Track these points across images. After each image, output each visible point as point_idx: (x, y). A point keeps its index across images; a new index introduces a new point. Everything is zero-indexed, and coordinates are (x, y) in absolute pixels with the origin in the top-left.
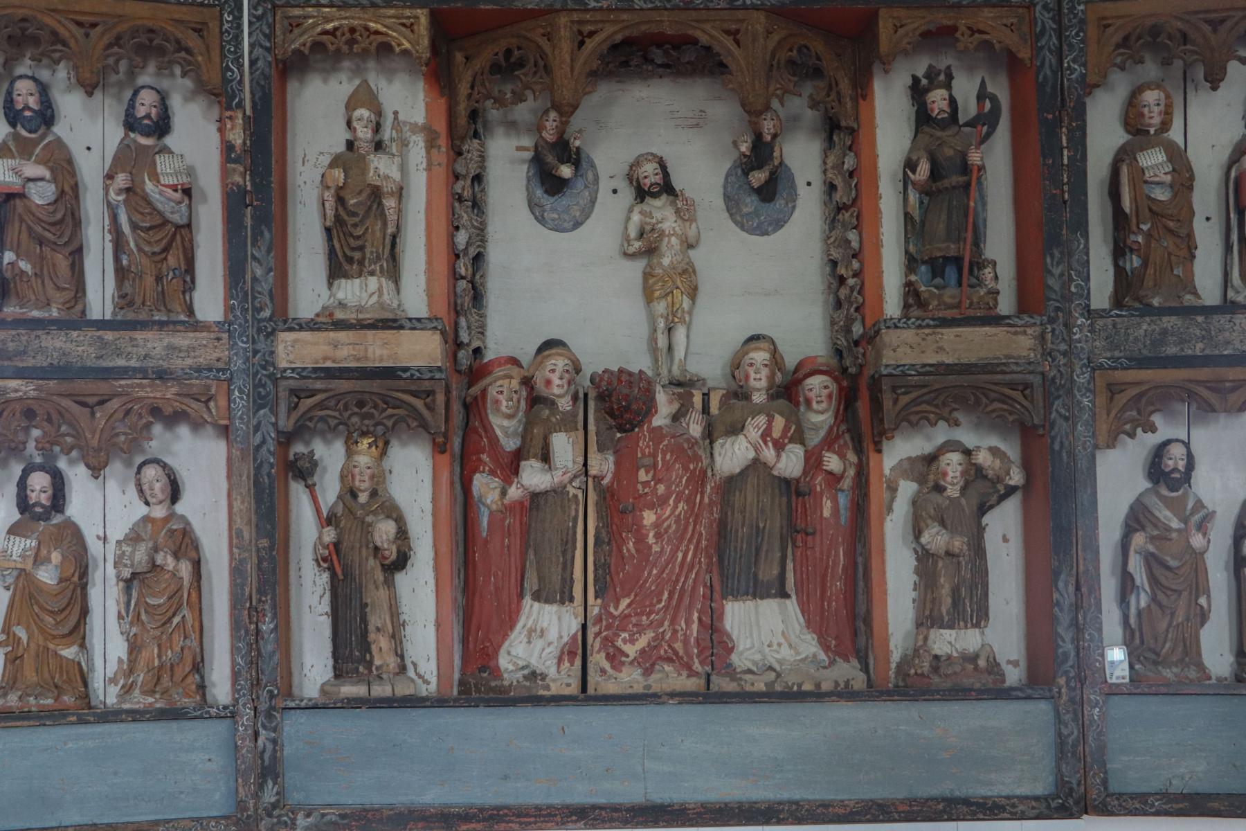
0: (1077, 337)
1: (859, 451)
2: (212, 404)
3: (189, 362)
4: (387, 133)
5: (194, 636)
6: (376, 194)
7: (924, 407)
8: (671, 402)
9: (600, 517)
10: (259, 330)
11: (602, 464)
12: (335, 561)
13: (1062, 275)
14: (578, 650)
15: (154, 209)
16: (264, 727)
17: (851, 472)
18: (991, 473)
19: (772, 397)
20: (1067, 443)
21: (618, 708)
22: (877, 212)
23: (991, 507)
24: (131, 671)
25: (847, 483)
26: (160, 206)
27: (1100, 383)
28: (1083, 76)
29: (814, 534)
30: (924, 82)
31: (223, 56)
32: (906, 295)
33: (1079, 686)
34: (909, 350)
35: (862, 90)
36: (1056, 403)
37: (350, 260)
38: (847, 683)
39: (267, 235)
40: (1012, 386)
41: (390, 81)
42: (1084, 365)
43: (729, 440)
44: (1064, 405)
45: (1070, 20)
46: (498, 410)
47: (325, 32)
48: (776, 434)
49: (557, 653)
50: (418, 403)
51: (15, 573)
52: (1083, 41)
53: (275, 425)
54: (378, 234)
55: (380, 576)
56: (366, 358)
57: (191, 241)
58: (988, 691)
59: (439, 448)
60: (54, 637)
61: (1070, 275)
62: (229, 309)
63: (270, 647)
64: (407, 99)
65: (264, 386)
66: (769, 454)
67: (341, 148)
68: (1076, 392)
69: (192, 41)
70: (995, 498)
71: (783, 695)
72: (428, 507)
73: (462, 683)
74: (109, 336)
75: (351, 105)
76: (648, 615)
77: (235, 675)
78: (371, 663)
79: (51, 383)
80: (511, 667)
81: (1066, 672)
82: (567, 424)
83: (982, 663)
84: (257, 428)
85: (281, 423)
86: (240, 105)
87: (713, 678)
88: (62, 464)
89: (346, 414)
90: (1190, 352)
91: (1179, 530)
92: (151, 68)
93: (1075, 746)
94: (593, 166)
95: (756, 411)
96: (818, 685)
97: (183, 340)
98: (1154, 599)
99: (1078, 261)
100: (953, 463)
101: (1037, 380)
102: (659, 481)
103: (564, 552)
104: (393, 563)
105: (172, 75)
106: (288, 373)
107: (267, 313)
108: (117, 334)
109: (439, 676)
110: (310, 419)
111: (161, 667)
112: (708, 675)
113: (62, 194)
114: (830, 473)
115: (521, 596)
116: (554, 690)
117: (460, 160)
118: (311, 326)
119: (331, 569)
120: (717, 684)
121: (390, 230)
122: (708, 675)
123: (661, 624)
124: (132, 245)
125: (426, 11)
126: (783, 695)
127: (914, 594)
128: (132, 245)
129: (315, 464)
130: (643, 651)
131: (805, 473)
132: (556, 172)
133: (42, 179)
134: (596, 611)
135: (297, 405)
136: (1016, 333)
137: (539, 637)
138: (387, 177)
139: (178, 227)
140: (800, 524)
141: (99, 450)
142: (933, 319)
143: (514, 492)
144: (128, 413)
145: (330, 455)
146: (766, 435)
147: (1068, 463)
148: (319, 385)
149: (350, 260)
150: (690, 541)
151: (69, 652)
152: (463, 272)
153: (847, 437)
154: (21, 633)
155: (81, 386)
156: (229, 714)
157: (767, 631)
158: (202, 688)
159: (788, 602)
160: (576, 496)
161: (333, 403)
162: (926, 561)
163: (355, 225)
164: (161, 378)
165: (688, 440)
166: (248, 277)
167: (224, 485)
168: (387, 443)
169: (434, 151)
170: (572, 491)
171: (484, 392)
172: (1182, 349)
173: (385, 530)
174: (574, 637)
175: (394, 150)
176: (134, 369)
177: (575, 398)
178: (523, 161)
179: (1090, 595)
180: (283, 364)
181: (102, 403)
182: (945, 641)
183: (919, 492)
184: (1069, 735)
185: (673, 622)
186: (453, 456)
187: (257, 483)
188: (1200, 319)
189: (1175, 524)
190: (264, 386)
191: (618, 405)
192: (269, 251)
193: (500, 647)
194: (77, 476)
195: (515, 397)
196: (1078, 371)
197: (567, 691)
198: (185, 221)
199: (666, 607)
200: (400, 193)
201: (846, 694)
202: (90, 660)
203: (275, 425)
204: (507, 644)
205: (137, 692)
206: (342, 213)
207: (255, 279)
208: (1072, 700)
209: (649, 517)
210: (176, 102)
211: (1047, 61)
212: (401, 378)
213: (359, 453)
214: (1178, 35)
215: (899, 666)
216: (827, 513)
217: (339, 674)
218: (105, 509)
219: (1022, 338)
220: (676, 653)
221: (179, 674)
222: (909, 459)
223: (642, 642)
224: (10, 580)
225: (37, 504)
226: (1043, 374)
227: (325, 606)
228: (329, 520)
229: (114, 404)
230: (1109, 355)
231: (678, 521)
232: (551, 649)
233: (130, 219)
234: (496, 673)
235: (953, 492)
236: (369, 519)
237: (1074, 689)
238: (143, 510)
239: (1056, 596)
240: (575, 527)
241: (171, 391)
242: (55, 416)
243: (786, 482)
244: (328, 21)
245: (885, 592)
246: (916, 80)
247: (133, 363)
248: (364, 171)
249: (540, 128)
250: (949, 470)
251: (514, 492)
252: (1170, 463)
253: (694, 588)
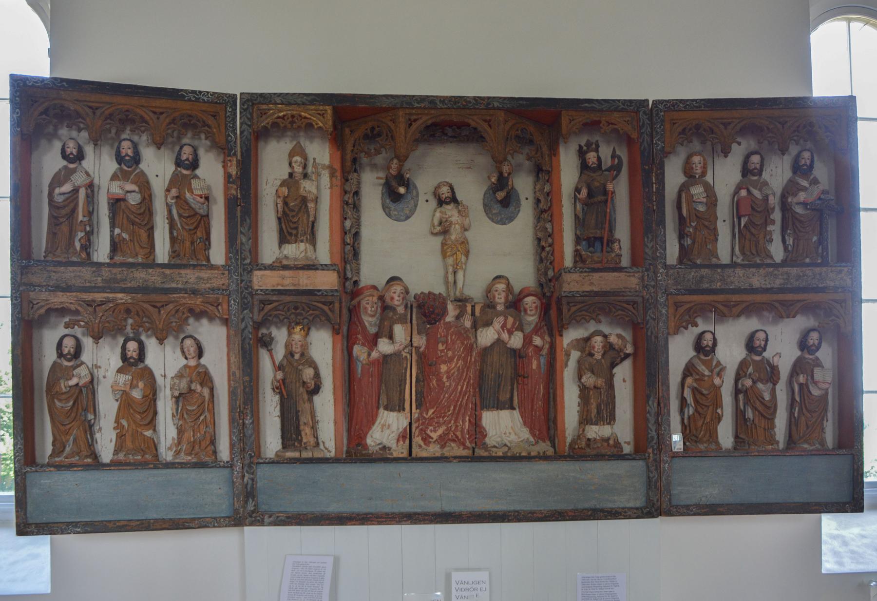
1: (551, 335)
2: (220, 307)
3: (208, 285)
4: (310, 169)
5: (211, 426)
6: (304, 200)
7: (584, 313)
8: (455, 309)
9: (418, 368)
10: (244, 270)
11: (420, 341)
12: (283, 389)
13: (652, 247)
14: (407, 435)
15: (191, 207)
16: (247, 472)
17: (547, 346)
18: (617, 347)
19: (507, 308)
21: (428, 464)
22: (561, 214)
23: (617, 364)
24: (179, 443)
25: (544, 352)
26: (193, 206)
29: (527, 377)
30: (585, 148)
31: (226, 129)
32: (575, 256)
35: (554, 151)
37: (291, 234)
38: (544, 453)
39: (248, 220)
40: (628, 303)
41: (311, 143)
43: (485, 329)
46: (367, 312)
47: (279, 117)
48: (509, 326)
49: (396, 437)
50: (326, 308)
51: (121, 393)
52: (663, 130)
53: (252, 318)
54: (305, 221)
55: (306, 397)
56: (299, 285)
57: (209, 223)
58: (613, 456)
59: (336, 331)
60: (141, 425)
62: (228, 258)
63: (250, 432)
64: (320, 152)
65: (246, 298)
66: (505, 336)
67: (286, 176)
69: (211, 121)
70: (619, 360)
71: (512, 457)
72: (330, 362)
73: (347, 452)
74: (168, 272)
75: (291, 155)
76: (443, 418)
77: (232, 446)
78: (301, 440)
79: (139, 295)
80: (373, 444)
81: (652, 447)
82: (402, 320)
83: (611, 442)
84: (243, 320)
85: (255, 317)
86: (235, 154)
87: (476, 450)
88: (143, 338)
89: (288, 314)
91: (708, 376)
92: (189, 135)
93: (656, 482)
94: (416, 187)
95: (498, 314)
96: (529, 453)
97: (205, 274)
98: (696, 410)
100: (598, 341)
101: (640, 300)
102: (449, 350)
103: (400, 385)
104: (312, 390)
105: (200, 138)
106: (259, 292)
107: (248, 261)
108: (172, 271)
109: (336, 448)
110: (270, 316)
111: (194, 442)
112: (474, 449)
113: (144, 199)
114: (536, 346)
115: (378, 408)
116: (395, 455)
117: (348, 184)
118: (271, 267)
119: (281, 393)
120: (479, 452)
121: (311, 219)
122: (474, 449)
123: (450, 422)
124: (179, 225)
125: (331, 107)
126: (512, 457)
127: (578, 409)
128: (179, 225)
129: (272, 339)
130: (440, 436)
131: (523, 346)
132: (397, 191)
133: (134, 191)
134: (417, 415)
135: (263, 308)
136: (629, 276)
137: (387, 428)
138: (310, 192)
139: (202, 216)
140: (521, 372)
141: (162, 330)
143: (375, 355)
144: (177, 311)
145: (280, 335)
146: (503, 327)
148: (275, 298)
149: (291, 234)
150: (465, 380)
151: (148, 433)
152: (348, 241)
153: (545, 328)
154: (124, 423)
155: (154, 297)
156: (230, 466)
157: (503, 426)
158: (215, 452)
159: (514, 412)
160: (406, 357)
161: (281, 308)
162: (585, 392)
163: (293, 216)
164: (193, 293)
165: (464, 329)
166: (238, 242)
167: (225, 350)
168: (309, 329)
169: (334, 179)
170: (404, 354)
171: (359, 303)
173: (308, 373)
174: (405, 429)
175: (314, 178)
176: (180, 289)
177: (406, 307)
178: (380, 185)
180: (256, 287)
181: (162, 306)
182: (594, 431)
183: (581, 356)
185: (456, 421)
186: (343, 335)
187: (243, 348)
188: (719, 270)
189: (707, 373)
190: (246, 298)
191: (428, 310)
192: (249, 230)
193: (367, 433)
194: (151, 344)
195: (375, 306)
196: (660, 295)
197: (401, 456)
198: (206, 213)
199: (453, 414)
200: (316, 200)
201: (544, 457)
202: (158, 438)
203: (252, 318)
204: (371, 432)
205: (182, 454)
206: (286, 209)
207: (242, 243)
208: (655, 460)
209: (444, 368)
210: (201, 152)
212: (316, 295)
213: (295, 333)
215: (570, 445)
216: (534, 367)
217: (285, 446)
218: (164, 360)
219: (632, 279)
220: (457, 437)
221: (203, 445)
222: (577, 340)
223: (440, 431)
224: (118, 396)
225: (131, 357)
226: (643, 297)
227: (277, 412)
228: (280, 368)
229: (171, 306)
231: (458, 370)
232: (393, 435)
233: (178, 212)
234: (366, 447)
235: (598, 356)
236: (300, 367)
238: (184, 362)
239: (648, 408)
240: (406, 373)
241: (199, 301)
242: (141, 313)
243: (514, 352)
244: (280, 111)
245: (563, 407)
246: (580, 147)
247: (179, 286)
248: (298, 188)
249: (389, 168)
250: (596, 345)
251: (375, 355)
252: (705, 342)
253: (467, 404)
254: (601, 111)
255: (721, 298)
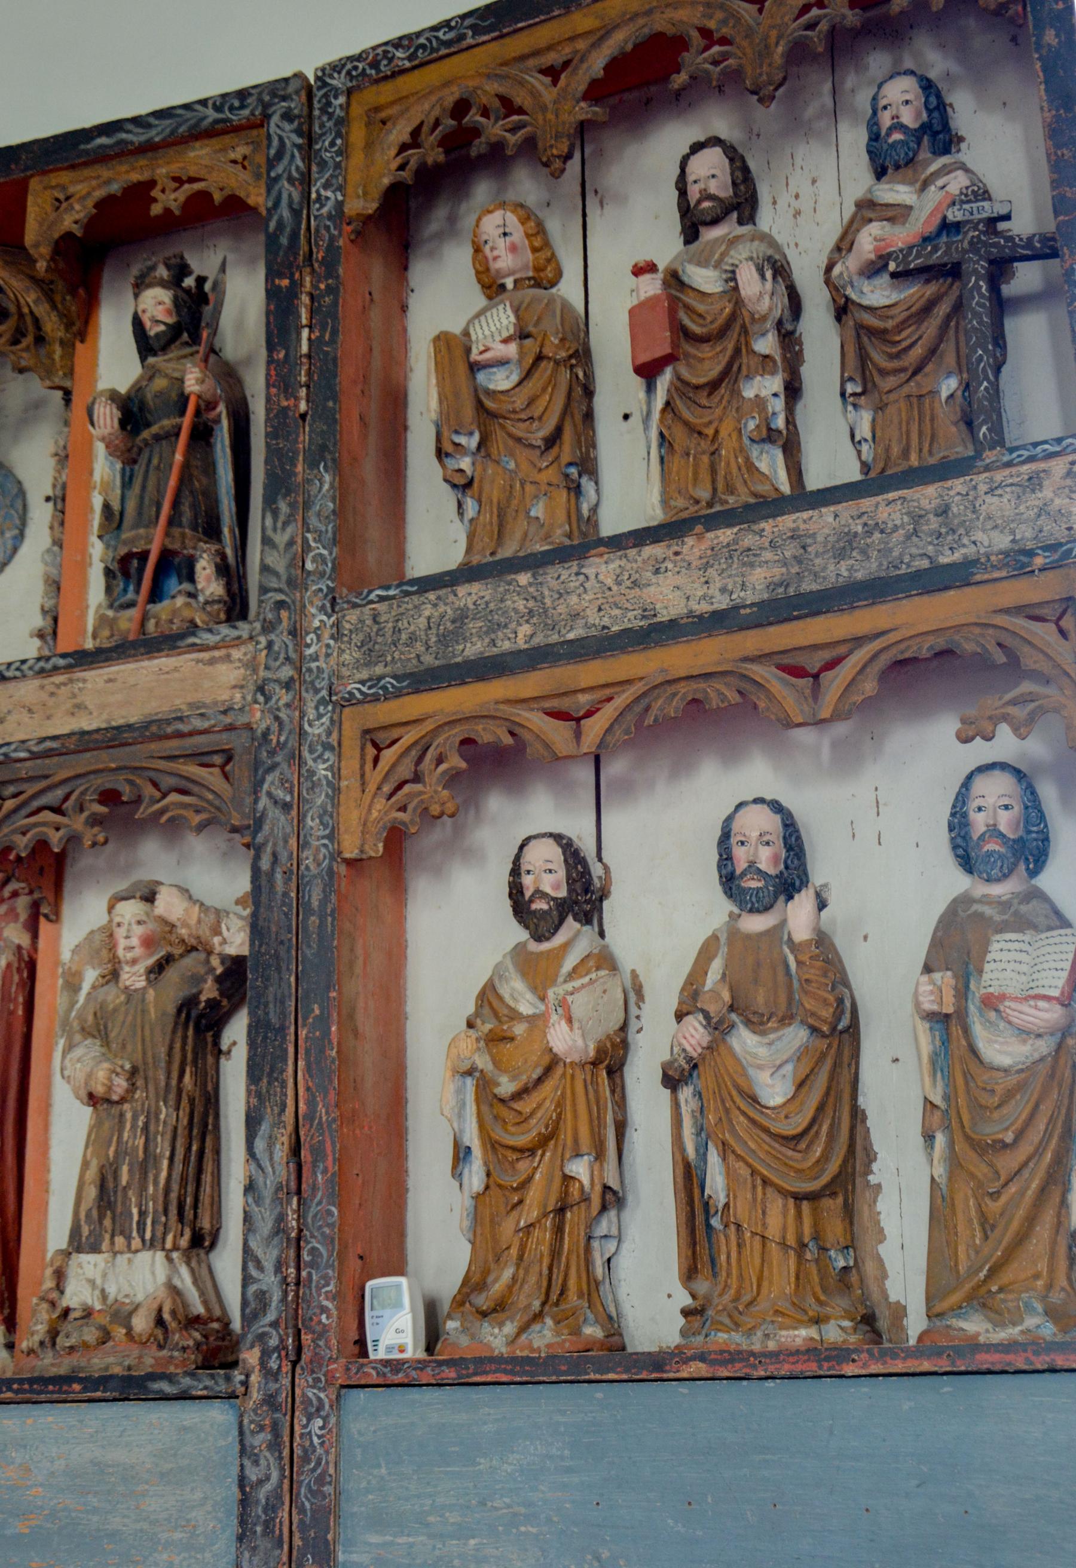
0: (309, 652)
13: (291, 543)
20: (283, 856)
27: (351, 730)
28: (340, 205)
33: (287, 1368)
34: (25, 717)
36: (269, 778)
42: (322, 702)
44: (282, 781)
45: (322, 126)
52: (339, 153)
61: (305, 541)
68: (306, 754)
81: (262, 1337)
90: (506, 646)
91: (532, 1019)
93: (271, 1508)
99: (319, 514)
136: (212, 662)
142: (64, 656)
147: (285, 894)
172: (493, 643)
179: (314, 1166)
184: (260, 1482)
188: (524, 578)
196: (311, 714)
208: (270, 1401)
211: (285, 196)
214: (497, 103)
219: (222, 668)
230: (364, 674)
237: (275, 1375)
254: (148, 148)
255: (530, 684)
